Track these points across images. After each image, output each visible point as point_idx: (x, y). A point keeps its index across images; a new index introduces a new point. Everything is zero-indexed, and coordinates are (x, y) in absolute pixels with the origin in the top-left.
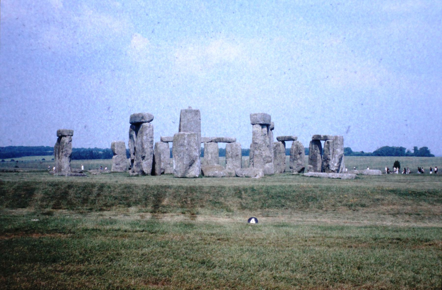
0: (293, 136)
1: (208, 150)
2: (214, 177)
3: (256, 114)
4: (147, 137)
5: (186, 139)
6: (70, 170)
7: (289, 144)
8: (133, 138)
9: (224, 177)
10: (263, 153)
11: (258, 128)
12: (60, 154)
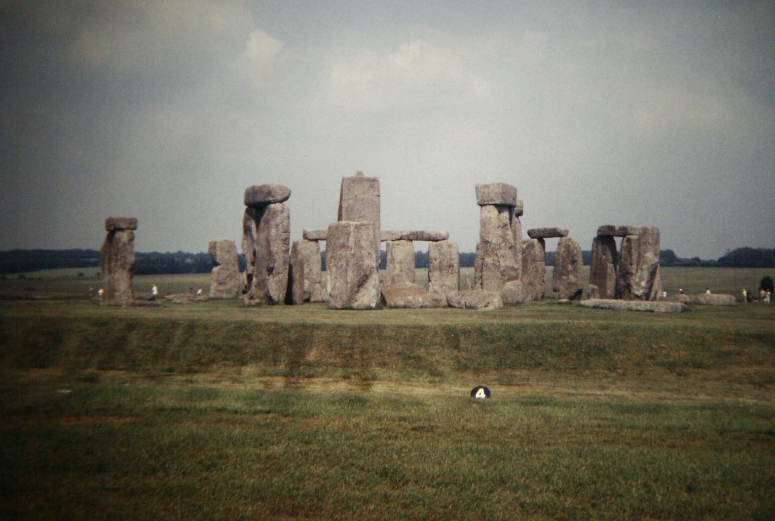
0: (561, 228)
1: (395, 256)
2: (405, 307)
3: (487, 186)
4: (278, 231)
5: (352, 234)
6: (130, 294)
8: (251, 232)
9: (426, 307)
10: (501, 260)
11: (492, 212)
12: (113, 264)
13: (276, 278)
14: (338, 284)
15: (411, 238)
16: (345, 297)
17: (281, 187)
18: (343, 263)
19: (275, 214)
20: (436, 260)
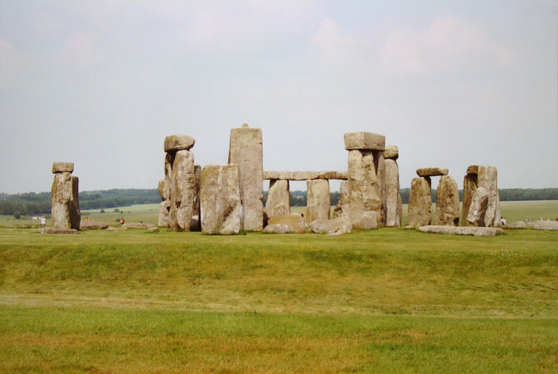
0: (441, 168)
1: (314, 191)
2: (273, 233)
3: (353, 135)
5: (220, 174)
7: (435, 180)
10: (364, 194)
11: (358, 155)
13: (183, 210)
14: (208, 214)
15: (327, 177)
16: (214, 225)
17: (186, 138)
18: (212, 197)
19: (181, 158)
20: (346, 195)
